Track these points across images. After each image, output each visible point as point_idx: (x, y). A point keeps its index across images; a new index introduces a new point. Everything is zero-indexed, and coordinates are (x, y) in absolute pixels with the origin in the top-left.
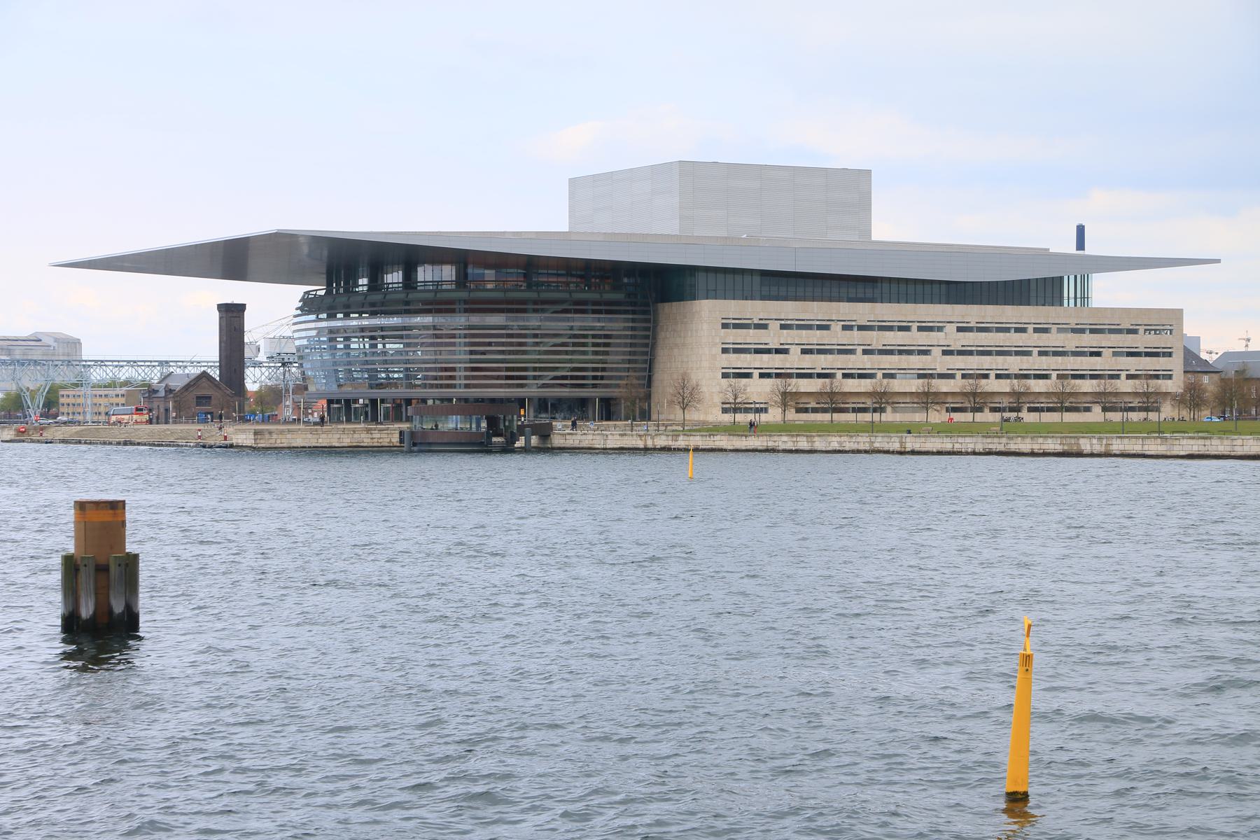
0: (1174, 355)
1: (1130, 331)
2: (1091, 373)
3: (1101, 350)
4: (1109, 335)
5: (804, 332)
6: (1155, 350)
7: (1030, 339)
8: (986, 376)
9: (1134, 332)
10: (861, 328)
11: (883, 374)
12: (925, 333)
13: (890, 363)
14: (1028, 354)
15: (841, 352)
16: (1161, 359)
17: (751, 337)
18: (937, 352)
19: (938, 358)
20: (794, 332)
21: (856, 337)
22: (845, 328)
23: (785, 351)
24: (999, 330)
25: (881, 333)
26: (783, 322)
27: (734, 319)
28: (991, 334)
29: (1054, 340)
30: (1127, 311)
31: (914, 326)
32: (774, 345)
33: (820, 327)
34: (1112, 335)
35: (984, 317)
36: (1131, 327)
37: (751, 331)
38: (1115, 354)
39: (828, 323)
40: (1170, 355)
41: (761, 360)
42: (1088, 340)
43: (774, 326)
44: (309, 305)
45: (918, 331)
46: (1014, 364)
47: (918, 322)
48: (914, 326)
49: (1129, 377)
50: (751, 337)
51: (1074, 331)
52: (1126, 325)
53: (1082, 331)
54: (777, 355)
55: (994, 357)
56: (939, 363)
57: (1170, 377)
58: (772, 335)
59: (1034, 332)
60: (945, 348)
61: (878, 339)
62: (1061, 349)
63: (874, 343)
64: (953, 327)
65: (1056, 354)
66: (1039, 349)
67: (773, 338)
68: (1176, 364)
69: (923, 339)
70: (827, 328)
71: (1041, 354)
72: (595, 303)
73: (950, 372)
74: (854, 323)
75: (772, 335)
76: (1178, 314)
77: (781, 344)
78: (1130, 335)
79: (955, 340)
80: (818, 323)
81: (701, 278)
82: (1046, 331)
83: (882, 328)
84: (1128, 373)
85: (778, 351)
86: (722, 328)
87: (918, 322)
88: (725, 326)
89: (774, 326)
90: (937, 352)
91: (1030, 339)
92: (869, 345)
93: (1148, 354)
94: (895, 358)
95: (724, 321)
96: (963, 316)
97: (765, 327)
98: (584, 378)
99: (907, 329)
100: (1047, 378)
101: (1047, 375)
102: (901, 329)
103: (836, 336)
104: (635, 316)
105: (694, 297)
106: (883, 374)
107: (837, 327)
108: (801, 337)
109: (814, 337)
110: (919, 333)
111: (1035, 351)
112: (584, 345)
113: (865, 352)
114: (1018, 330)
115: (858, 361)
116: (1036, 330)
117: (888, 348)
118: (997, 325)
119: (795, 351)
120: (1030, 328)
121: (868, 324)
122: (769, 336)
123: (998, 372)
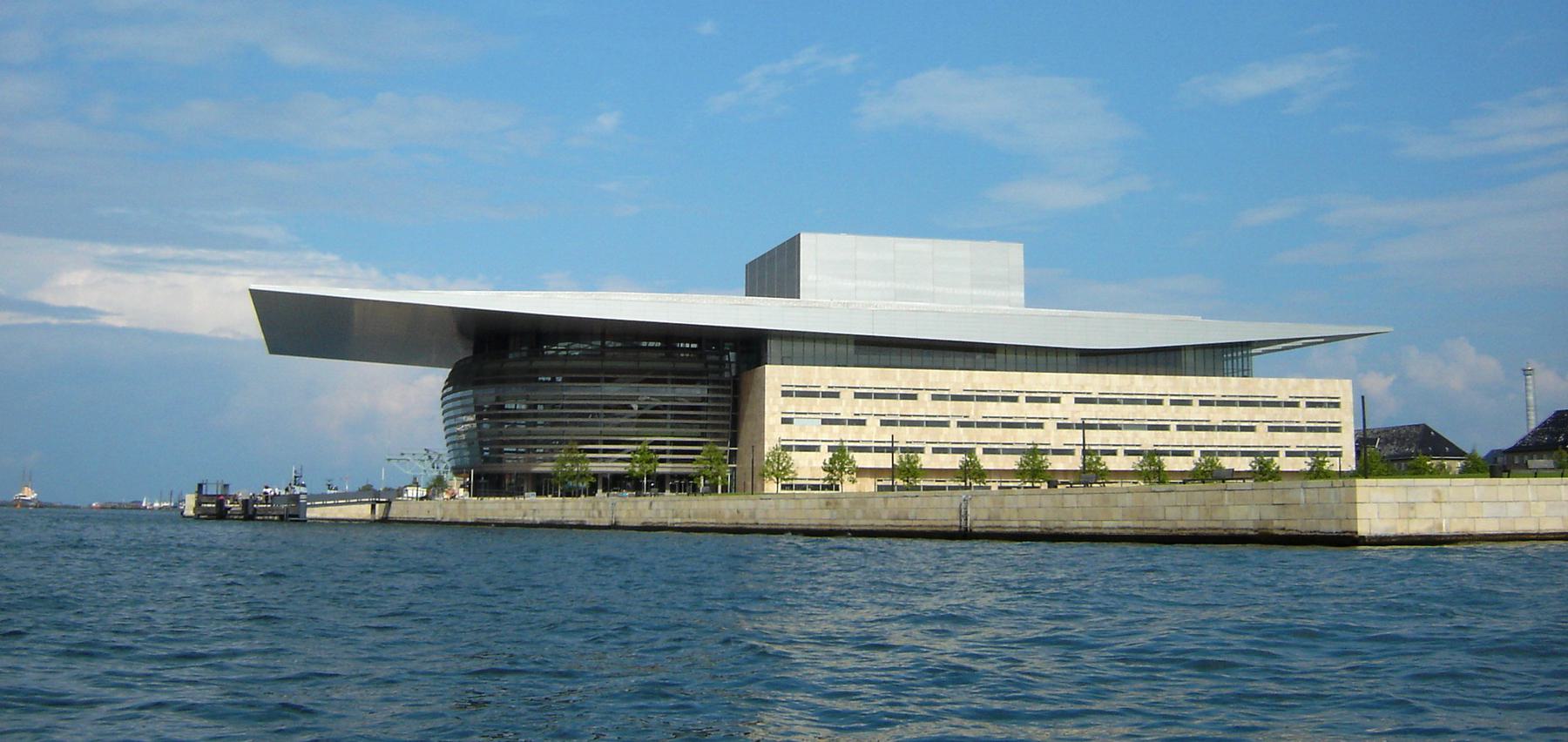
0: (1343, 431)
1: (1288, 404)
2: (1243, 449)
3: (1254, 424)
4: (1263, 408)
5: (884, 401)
6: (1320, 425)
7: (1165, 412)
8: (1114, 453)
9: (1295, 405)
10: (956, 398)
11: (984, 449)
12: (1036, 404)
13: (992, 438)
14: (1165, 428)
15: (929, 424)
16: (1329, 435)
18: (1050, 426)
19: (1053, 433)
20: (873, 401)
21: (949, 408)
22: (935, 398)
23: (862, 423)
24: (1127, 402)
25: (980, 403)
26: (857, 391)
27: (797, 386)
28: (1117, 406)
29: (1195, 413)
31: (1022, 398)
32: (847, 415)
33: (905, 397)
34: (1267, 408)
35: (1109, 387)
36: (1290, 400)
37: (819, 400)
38: (1271, 429)
39: (915, 392)
40: (1336, 430)
41: (831, 432)
42: (1238, 414)
43: (847, 395)
45: (1027, 401)
46: (1148, 440)
47: (1027, 392)
48: (1022, 398)
49: (1289, 454)
51: (1221, 403)
52: (1283, 398)
53: (1232, 403)
54: (851, 427)
55: (1123, 432)
56: (1051, 437)
57: (1338, 454)
58: (844, 404)
59: (1171, 404)
60: (1060, 421)
61: (975, 411)
62: (1204, 423)
63: (972, 413)
64: (1071, 398)
65: (1199, 428)
66: (1177, 423)
67: (845, 407)
68: (1346, 442)
70: (914, 397)
71: (1180, 428)
72: (674, 372)
73: (1067, 447)
74: (946, 393)
75: (844, 404)
77: (855, 415)
78: (1289, 408)
79: (1073, 412)
80: (902, 392)
81: (773, 347)
82: (1188, 403)
83: (981, 399)
84: (1287, 449)
85: (852, 422)
86: (783, 396)
87: (1027, 392)
88: (785, 394)
89: (847, 395)
90: (1050, 426)
91: (1165, 412)
92: (965, 417)
93: (1311, 429)
94: (999, 432)
95: (785, 389)
96: (1083, 387)
97: (836, 395)
98: (675, 452)
99: (1015, 399)
100: (1190, 455)
101: (1190, 451)
102: (1005, 399)
103: (925, 407)
104: (717, 387)
105: (767, 364)
106: (984, 449)
107: (925, 397)
108: (881, 407)
109: (897, 408)
110: (1028, 404)
111: (1173, 425)
112: (665, 416)
113: (961, 424)
114: (1151, 402)
115: (953, 435)
116: (1173, 403)
117: (990, 420)
118: (1124, 397)
119: (873, 423)
120: (1167, 400)
121: (964, 393)
122: (841, 405)
123: (1128, 448)
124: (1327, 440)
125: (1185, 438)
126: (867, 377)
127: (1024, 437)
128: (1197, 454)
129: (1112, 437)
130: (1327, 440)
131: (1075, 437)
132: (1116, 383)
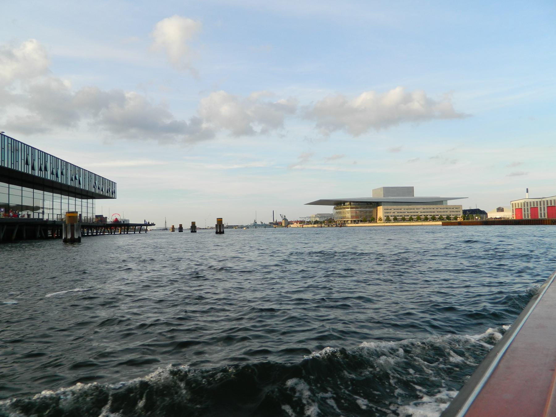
7: (435, 210)
17: (389, 211)
29: (439, 210)
30: (452, 206)
42: (445, 210)
44: (335, 208)
46: (433, 214)
50: (389, 211)
56: (420, 214)
61: (409, 211)
68: (461, 213)
69: (417, 210)
76: (461, 206)
103: (403, 210)
109: (399, 211)
124: (459, 213)
125: (438, 213)
126: (395, 207)
127: (416, 214)
128: (439, 215)
129: (428, 214)
130: (459, 213)
131: (423, 214)
132: (428, 206)
